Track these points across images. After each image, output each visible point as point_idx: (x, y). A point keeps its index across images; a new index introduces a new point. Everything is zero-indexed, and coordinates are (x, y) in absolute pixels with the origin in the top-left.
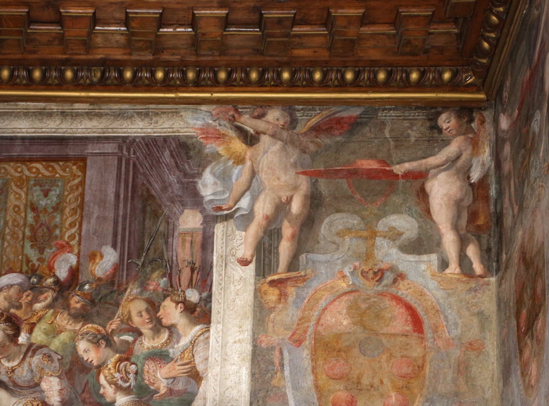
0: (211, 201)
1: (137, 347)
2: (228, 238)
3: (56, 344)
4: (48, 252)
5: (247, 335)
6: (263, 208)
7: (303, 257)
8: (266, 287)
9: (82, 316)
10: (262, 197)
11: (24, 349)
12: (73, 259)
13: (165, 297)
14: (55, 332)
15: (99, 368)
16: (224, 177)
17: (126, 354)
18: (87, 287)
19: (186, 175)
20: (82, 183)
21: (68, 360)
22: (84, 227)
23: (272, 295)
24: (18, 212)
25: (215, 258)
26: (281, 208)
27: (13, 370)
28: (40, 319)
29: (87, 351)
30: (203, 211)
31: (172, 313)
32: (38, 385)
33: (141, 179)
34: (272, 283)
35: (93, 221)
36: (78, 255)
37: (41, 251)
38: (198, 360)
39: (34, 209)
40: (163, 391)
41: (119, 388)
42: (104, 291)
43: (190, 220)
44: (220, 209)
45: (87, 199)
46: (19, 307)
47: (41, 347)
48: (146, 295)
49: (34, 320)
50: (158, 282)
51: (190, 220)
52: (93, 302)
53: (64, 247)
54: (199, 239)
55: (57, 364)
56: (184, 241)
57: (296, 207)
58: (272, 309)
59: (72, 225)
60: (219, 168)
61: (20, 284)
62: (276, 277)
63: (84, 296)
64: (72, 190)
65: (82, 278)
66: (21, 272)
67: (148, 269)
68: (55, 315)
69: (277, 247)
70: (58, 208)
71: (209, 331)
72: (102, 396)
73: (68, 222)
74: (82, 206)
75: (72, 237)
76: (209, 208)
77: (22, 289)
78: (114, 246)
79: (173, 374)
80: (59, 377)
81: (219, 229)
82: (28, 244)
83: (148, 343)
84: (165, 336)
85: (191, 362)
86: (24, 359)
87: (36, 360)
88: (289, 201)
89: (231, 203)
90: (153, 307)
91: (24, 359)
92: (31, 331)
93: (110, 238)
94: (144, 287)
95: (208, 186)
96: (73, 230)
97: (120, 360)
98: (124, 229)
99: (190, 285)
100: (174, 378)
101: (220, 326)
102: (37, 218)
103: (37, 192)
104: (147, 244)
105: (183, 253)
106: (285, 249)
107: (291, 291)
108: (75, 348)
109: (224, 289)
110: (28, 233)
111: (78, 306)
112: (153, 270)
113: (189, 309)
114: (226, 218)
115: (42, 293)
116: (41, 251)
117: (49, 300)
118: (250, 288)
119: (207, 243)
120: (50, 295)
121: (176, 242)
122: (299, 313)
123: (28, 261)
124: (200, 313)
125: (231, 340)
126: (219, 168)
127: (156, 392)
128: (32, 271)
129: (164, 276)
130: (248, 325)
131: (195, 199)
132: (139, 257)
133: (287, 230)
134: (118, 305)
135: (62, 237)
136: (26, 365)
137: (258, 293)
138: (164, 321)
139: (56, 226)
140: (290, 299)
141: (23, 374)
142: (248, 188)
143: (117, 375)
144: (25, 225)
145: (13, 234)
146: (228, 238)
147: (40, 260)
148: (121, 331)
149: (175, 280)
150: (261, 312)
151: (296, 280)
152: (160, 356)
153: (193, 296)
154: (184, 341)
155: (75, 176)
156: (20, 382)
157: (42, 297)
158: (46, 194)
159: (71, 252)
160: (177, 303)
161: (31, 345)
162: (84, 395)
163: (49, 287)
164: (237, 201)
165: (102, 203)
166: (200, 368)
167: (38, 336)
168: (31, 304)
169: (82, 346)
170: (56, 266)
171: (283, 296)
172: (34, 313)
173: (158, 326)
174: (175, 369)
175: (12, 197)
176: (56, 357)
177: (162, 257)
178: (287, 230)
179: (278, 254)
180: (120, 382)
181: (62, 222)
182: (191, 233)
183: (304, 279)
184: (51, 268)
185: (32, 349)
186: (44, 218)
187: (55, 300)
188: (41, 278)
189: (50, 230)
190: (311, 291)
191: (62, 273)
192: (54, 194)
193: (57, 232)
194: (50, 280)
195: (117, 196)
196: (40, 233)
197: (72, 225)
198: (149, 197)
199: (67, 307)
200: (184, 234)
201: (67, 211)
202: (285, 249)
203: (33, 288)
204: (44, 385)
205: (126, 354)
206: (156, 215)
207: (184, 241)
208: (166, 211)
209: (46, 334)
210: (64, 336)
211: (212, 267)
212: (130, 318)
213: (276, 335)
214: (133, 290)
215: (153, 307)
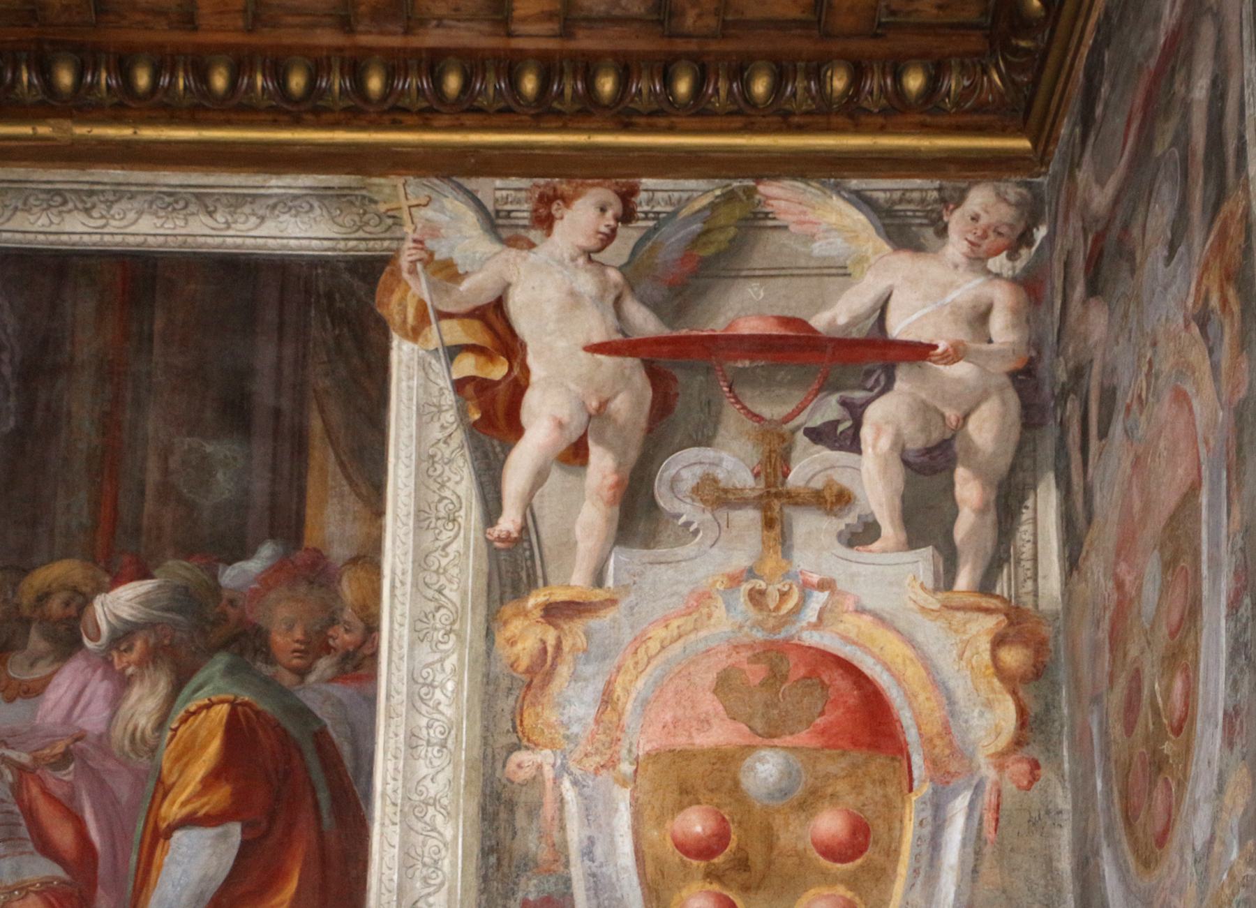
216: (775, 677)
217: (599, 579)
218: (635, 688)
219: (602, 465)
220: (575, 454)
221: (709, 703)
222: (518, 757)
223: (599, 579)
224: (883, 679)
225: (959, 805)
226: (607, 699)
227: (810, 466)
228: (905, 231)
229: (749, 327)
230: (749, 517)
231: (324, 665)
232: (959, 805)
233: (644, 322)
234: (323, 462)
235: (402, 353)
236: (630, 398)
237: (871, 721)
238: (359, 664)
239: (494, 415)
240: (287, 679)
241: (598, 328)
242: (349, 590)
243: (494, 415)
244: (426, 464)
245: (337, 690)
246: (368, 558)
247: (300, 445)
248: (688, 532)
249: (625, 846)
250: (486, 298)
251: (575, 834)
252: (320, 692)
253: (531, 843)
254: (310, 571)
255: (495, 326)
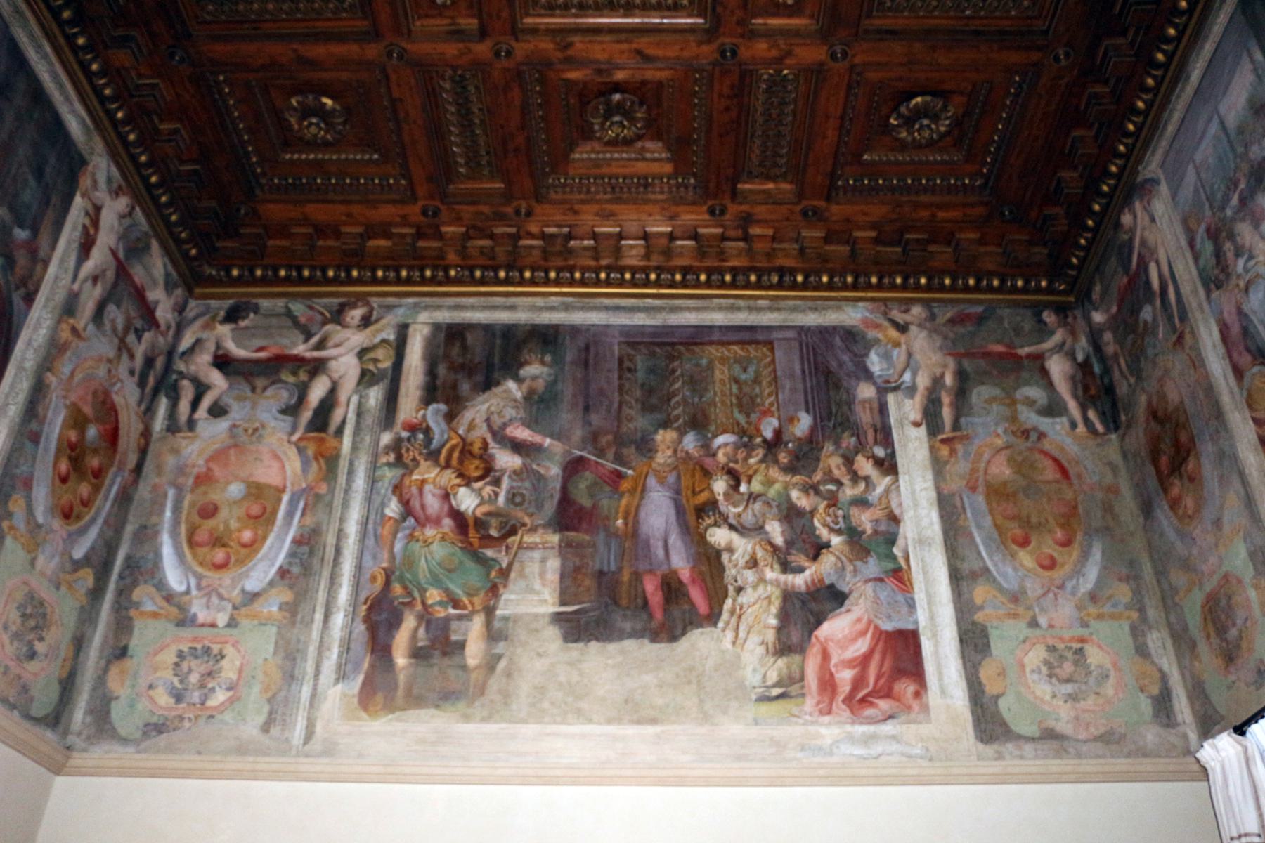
0: (880, 376)
1: (840, 495)
2: (899, 405)
3: (772, 492)
4: (754, 417)
5: (930, 483)
6: (923, 381)
7: (963, 420)
8: (938, 444)
9: (790, 469)
10: (920, 373)
11: (746, 497)
12: (775, 423)
13: (857, 453)
14: (769, 483)
15: (813, 512)
16: (886, 356)
17: (833, 501)
18: (790, 445)
19: (855, 355)
20: (773, 361)
21: (784, 506)
22: (780, 396)
23: (945, 451)
24: (724, 385)
25: (892, 421)
26: (937, 382)
27: (739, 515)
28: (756, 472)
29: (801, 500)
30: (875, 383)
31: (865, 466)
32: (762, 527)
33: (820, 358)
34: (943, 441)
35: (787, 391)
36: (779, 418)
37: (748, 416)
38: (894, 505)
39: (737, 381)
40: (869, 532)
41: (832, 530)
42: (805, 449)
43: (866, 391)
44: (888, 382)
45: (779, 373)
46: (736, 462)
47: (759, 495)
48: (841, 451)
49: (751, 472)
50: (849, 441)
51: (866, 391)
52: (797, 458)
53: (766, 413)
54: (876, 405)
55: (775, 510)
56: (864, 408)
57: (949, 380)
58: (946, 463)
59: (770, 395)
60: (881, 350)
61: (734, 443)
62: (944, 436)
63: (789, 452)
64: (765, 367)
65: (785, 438)
66: (733, 433)
67: (839, 430)
68: (767, 468)
69: (940, 412)
70: (756, 381)
71: (897, 480)
72: (819, 537)
73: (767, 391)
74: (775, 379)
75: (771, 404)
76: (879, 381)
77: (737, 447)
78: (807, 411)
79: (875, 517)
80: (780, 520)
81: (891, 398)
82: (736, 411)
83: (849, 492)
84: (862, 485)
85: (888, 507)
86: (747, 506)
87: (757, 506)
88: (942, 376)
89: (896, 377)
90: (849, 461)
91: (747, 506)
92: (749, 482)
93: (803, 406)
94: (837, 444)
95: (875, 363)
96: (772, 399)
97: (829, 506)
98: (813, 398)
99: (876, 443)
100: (877, 521)
101: (907, 477)
102: (740, 389)
103: (737, 369)
104: (834, 410)
105: (865, 417)
106: (947, 413)
107: (959, 447)
108: (788, 497)
109: (905, 446)
110: (734, 401)
111: (786, 461)
112: (843, 432)
113: (879, 463)
114: (896, 389)
115: (753, 450)
116: (748, 416)
117: (760, 456)
118: (926, 445)
119: (883, 409)
120: (760, 452)
121: (858, 408)
122: (970, 466)
123: (738, 424)
124: (888, 466)
125: (918, 488)
126: (881, 350)
127: (864, 532)
128: (742, 433)
129: (852, 435)
130: (930, 476)
131: (868, 376)
132: (829, 420)
133: (946, 400)
134: (818, 460)
135: (763, 404)
136: (750, 511)
137: (932, 449)
138: (860, 473)
139: (757, 396)
140: (960, 454)
141: (748, 519)
142: (908, 365)
143: (829, 519)
144: (731, 394)
145: (723, 402)
146: (899, 405)
147: (749, 423)
148: (825, 482)
149: (863, 440)
150: (938, 467)
151: (962, 438)
152: (862, 502)
153: (880, 452)
154: (879, 490)
155: (766, 356)
156: (747, 525)
157: (754, 453)
158: (745, 370)
159: (773, 416)
160: (868, 458)
161: (751, 494)
162: (804, 536)
163: (759, 446)
164: (901, 375)
165: (792, 376)
166: (897, 512)
167: (756, 486)
168: (746, 459)
169: (795, 494)
170: (762, 428)
171: (953, 452)
172: (750, 467)
173: (856, 478)
174: (878, 513)
175: (717, 373)
176: (774, 504)
177: (848, 420)
178: (946, 400)
179: (941, 418)
180: (832, 525)
181: (762, 392)
182: (869, 401)
183: (967, 437)
184: (758, 430)
185: (752, 497)
186: (746, 389)
187: (765, 456)
188: (751, 438)
189: (753, 399)
190: (975, 448)
191: (768, 434)
192: (751, 370)
193: (759, 400)
194: (759, 440)
195: (803, 372)
196: (745, 400)
197: (770, 395)
198: (828, 373)
199: (776, 462)
200: (864, 401)
201: (764, 383)
202: (947, 413)
203: (745, 446)
204: (768, 528)
205: (833, 501)
206: (837, 386)
207: (864, 408)
208: (845, 383)
209: (762, 484)
210: (777, 486)
211: (890, 428)
212: (830, 471)
213: (954, 484)
214: (829, 447)
215: (849, 461)
216: (104, 403)
217: (85, 329)
218: (79, 376)
219: (98, 291)
220: (95, 279)
221: (90, 398)
222: (49, 374)
223: (85, 329)
224: (121, 425)
225: (119, 479)
226: (72, 373)
227: (131, 338)
228: (169, 287)
229: (136, 279)
230: (116, 341)
231: (22, 291)
232: (119, 479)
233: (121, 255)
234: (51, 214)
235: (78, 200)
236: (110, 274)
237: (112, 436)
238: (29, 299)
239: (86, 246)
240: (13, 286)
241: (113, 244)
242: (39, 268)
243: (86, 246)
244: (69, 243)
245: (21, 303)
246: (46, 263)
247: (47, 203)
248: (104, 335)
249: (57, 430)
250: (99, 203)
251: (50, 415)
252: (17, 298)
253: (40, 410)
254: (33, 252)
255: (95, 213)
